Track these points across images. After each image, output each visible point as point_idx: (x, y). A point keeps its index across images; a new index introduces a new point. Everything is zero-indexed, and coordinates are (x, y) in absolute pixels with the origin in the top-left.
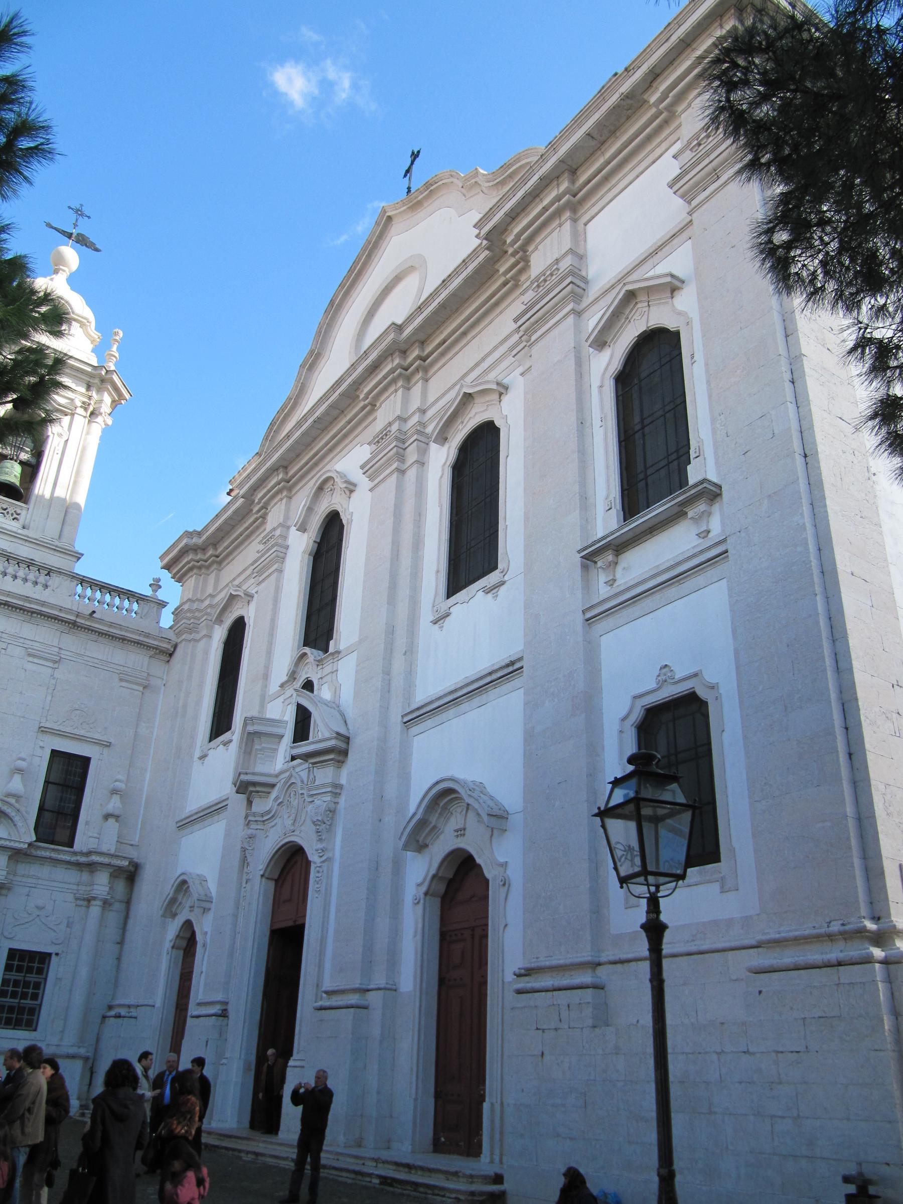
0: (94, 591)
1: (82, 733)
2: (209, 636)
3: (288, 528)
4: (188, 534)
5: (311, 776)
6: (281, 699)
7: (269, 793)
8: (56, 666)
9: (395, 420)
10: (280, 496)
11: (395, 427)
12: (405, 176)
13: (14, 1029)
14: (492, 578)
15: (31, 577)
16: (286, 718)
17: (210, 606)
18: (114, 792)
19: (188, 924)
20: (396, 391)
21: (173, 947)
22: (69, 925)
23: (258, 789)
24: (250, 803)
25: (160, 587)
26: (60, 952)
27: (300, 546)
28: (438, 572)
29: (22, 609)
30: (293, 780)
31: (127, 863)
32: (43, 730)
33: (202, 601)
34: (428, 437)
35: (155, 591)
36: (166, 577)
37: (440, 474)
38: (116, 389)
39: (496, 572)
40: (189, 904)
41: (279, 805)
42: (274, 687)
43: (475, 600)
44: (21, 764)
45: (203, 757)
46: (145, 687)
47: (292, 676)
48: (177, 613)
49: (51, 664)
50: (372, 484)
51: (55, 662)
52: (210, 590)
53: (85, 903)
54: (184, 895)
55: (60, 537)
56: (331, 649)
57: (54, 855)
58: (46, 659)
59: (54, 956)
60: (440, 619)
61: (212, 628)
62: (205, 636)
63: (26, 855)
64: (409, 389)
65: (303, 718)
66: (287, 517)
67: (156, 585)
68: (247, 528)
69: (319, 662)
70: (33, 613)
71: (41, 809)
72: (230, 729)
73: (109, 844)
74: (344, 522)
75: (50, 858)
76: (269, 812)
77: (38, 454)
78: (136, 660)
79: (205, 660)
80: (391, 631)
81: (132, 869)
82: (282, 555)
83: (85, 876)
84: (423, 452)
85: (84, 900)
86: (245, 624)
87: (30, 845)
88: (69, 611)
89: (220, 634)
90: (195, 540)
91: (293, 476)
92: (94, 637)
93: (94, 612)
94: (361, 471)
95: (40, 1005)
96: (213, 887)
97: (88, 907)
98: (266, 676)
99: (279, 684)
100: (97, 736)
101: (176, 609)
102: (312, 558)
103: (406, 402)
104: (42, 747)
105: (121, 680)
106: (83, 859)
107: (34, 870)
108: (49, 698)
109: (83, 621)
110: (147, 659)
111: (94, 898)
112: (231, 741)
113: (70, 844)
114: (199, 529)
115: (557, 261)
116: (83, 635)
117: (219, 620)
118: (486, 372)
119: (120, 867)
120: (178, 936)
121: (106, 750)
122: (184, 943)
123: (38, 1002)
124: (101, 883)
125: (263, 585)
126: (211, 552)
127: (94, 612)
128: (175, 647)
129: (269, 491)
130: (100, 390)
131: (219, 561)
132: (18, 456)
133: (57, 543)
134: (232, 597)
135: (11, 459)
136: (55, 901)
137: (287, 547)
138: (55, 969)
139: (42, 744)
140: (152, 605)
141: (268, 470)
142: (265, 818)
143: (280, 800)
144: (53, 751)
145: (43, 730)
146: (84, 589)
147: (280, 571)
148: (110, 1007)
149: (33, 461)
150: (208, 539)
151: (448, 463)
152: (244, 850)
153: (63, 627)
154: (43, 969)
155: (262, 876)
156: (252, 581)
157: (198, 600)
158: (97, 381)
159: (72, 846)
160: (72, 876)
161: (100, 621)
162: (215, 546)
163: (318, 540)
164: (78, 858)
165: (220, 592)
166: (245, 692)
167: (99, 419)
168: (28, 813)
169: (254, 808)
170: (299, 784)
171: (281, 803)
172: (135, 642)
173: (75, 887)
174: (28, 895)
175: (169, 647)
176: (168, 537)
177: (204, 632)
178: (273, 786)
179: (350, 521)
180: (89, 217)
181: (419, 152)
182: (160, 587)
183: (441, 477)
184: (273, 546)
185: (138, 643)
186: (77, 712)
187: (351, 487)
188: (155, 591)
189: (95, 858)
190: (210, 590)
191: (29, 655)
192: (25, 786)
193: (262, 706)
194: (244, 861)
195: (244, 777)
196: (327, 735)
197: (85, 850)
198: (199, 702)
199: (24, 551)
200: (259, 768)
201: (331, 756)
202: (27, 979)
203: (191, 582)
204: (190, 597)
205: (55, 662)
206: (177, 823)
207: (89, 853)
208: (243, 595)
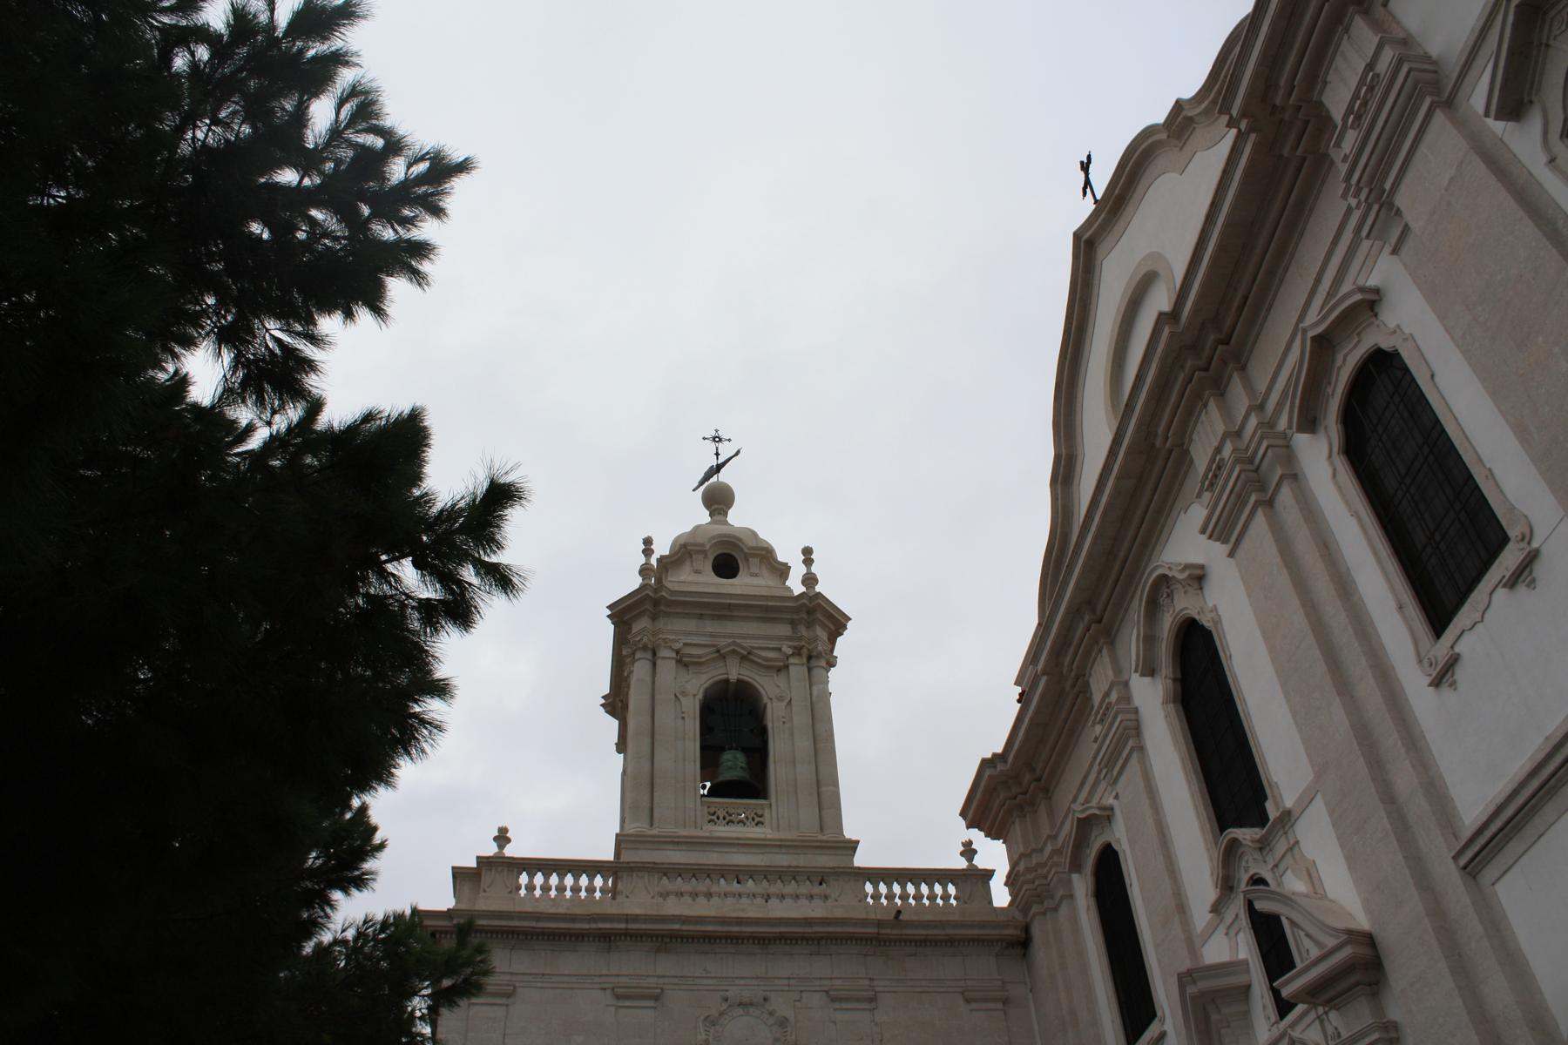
2: (1071, 896)
3: (1126, 684)
5: (1330, 1030)
6: (1222, 930)
8: (873, 1005)
9: (1222, 442)
11: (1227, 450)
12: (1085, 194)
14: (1509, 560)
16: (1242, 955)
17: (1055, 852)
20: (1205, 406)
25: (975, 852)
28: (1400, 607)
33: (1041, 850)
34: (1284, 435)
37: (1330, 471)
39: (1511, 546)
42: (1201, 915)
43: (1494, 619)
46: (1005, 1002)
47: (1227, 885)
48: (1011, 881)
50: (1226, 548)
52: (1046, 831)
55: (822, 829)
56: (1272, 812)
58: (858, 1000)
60: (1443, 675)
61: (1070, 882)
62: (1062, 898)
64: (1222, 395)
65: (1271, 937)
66: (1118, 670)
67: (969, 851)
69: (1263, 845)
70: (819, 940)
72: (1154, 1015)
74: (1207, 625)
80: (1364, 735)
84: (1289, 457)
86: (1115, 853)
89: (1082, 886)
90: (1000, 767)
94: (1204, 537)
98: (1182, 908)
99: (1208, 907)
101: (1008, 876)
103: (1226, 413)
112: (1163, 1035)
114: (999, 750)
115: (1370, 67)
117: (1076, 866)
118: (1330, 295)
125: (1123, 779)
126: (1027, 777)
128: (1027, 929)
130: (809, 625)
133: (820, 837)
137: (1136, 711)
141: (1068, 611)
147: (1141, 748)
150: (1016, 757)
151: (1335, 449)
156: (1103, 785)
157: (1034, 851)
165: (1063, 823)
166: (1157, 947)
177: (1060, 893)
179: (1218, 621)
181: (1089, 157)
182: (975, 852)
183: (1334, 475)
184: (1115, 718)
187: (1198, 572)
190: (1046, 831)
191: (833, 1000)
193: (1193, 951)
196: (1331, 942)
199: (783, 860)
201: (1352, 979)
203: (1017, 830)
204: (1022, 849)
205: (872, 1000)
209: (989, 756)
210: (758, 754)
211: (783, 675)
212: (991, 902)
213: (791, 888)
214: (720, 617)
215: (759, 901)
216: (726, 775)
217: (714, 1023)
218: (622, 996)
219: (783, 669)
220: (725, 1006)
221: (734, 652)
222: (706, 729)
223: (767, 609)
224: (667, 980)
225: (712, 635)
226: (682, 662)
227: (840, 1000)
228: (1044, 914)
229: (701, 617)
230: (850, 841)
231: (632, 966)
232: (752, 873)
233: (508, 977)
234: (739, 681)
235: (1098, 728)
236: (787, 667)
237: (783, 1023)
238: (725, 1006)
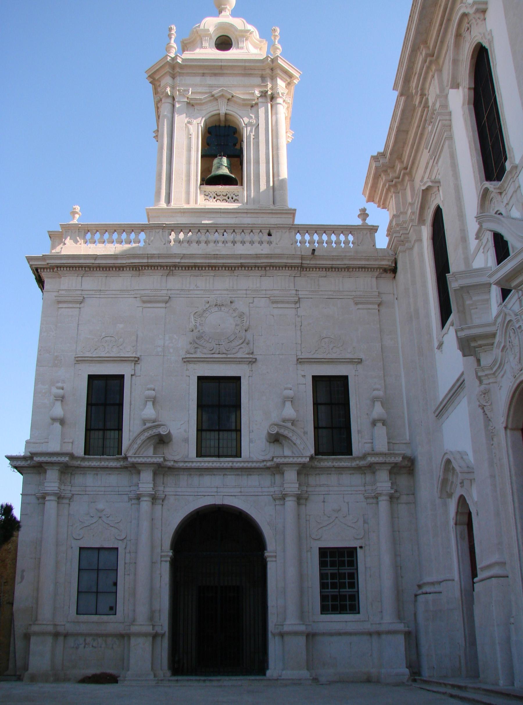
0: (311, 235)
1: (334, 356)
2: (420, 240)
3: (446, 96)
4: (375, 158)
7: (492, 344)
8: (298, 305)
10: (431, 74)
13: (340, 613)
15: (256, 238)
17: (413, 213)
18: (374, 400)
19: (462, 501)
21: (456, 524)
22: (365, 522)
23: (480, 342)
24: (478, 361)
25: (367, 215)
26: (363, 546)
27: (458, 102)
29: (257, 267)
30: (508, 319)
31: (401, 459)
32: (300, 361)
35: (364, 220)
36: (372, 208)
38: (286, 72)
40: (459, 481)
41: (502, 351)
44: (290, 393)
45: (440, 345)
49: (293, 306)
51: (296, 303)
53: (374, 501)
54: (453, 474)
57: (336, 464)
58: (288, 302)
59: (359, 550)
63: (312, 467)
67: (364, 214)
68: (418, 126)
71: (316, 428)
73: (382, 446)
75: (334, 467)
76: (495, 361)
78: (365, 283)
79: (422, 261)
81: (409, 464)
82: (447, 123)
83: (369, 478)
85: (373, 498)
86: (441, 209)
87: (311, 458)
88: (293, 257)
89: (426, 232)
91: (435, 46)
92: (324, 273)
93: (314, 250)
95: (358, 591)
96: (471, 457)
97: (377, 503)
98: (464, 239)
99: (475, 237)
100: (348, 356)
102: (472, 107)
104: (304, 376)
105: (356, 304)
106: (362, 463)
107: (323, 479)
108: (299, 333)
109: (308, 262)
110: (374, 280)
111: (380, 494)
113: (348, 451)
114: (382, 150)
116: (314, 274)
117: (421, 221)
119: (396, 464)
120: (457, 513)
121: (359, 366)
122: (466, 519)
123: (356, 590)
124: (383, 482)
126: (398, 166)
129: (420, 75)
131: (408, 172)
133: (272, 207)
134: (426, 192)
136: (348, 503)
137: (450, 114)
138: (363, 560)
139: (303, 374)
140: (365, 232)
142: (494, 369)
143: (502, 345)
144: (314, 377)
145: (300, 361)
146: (303, 236)
147: (451, 138)
148: (420, 586)
150: (391, 154)
152: (483, 407)
153: (294, 272)
154: (353, 561)
155: (506, 428)
157: (401, 213)
158: (268, 71)
159: (352, 455)
160: (357, 479)
161: (322, 258)
162: (400, 158)
163: (473, 86)
164: (358, 462)
167: (280, 100)
168: (305, 433)
169: (483, 363)
170: (513, 318)
171: (504, 347)
172: (359, 268)
173: (362, 488)
174: (324, 502)
175: (390, 263)
176: (360, 170)
178: (494, 335)
182: (367, 215)
185: (362, 268)
186: (326, 340)
188: (364, 220)
189: (371, 459)
190: (409, 200)
191: (273, 302)
192: (297, 411)
194: (487, 420)
195: (462, 334)
197: (361, 455)
198: (426, 301)
200: (476, 322)
202: (341, 571)
205: (296, 303)
206: (434, 412)
207: (364, 457)
208: (429, 184)
209: (375, 154)
210: (236, 157)
212: (374, 245)
213: (248, 238)
214: (215, 75)
215: (230, 245)
217: (201, 316)
218: (148, 301)
219: (254, 106)
220: (208, 305)
221: (222, 96)
223: (245, 68)
224: (173, 292)
225: (211, 86)
227: (277, 302)
228: (405, 251)
229: (203, 75)
230: (291, 210)
231: (151, 282)
233: (80, 292)
235: (430, 127)
237: (241, 315)
238: (208, 305)
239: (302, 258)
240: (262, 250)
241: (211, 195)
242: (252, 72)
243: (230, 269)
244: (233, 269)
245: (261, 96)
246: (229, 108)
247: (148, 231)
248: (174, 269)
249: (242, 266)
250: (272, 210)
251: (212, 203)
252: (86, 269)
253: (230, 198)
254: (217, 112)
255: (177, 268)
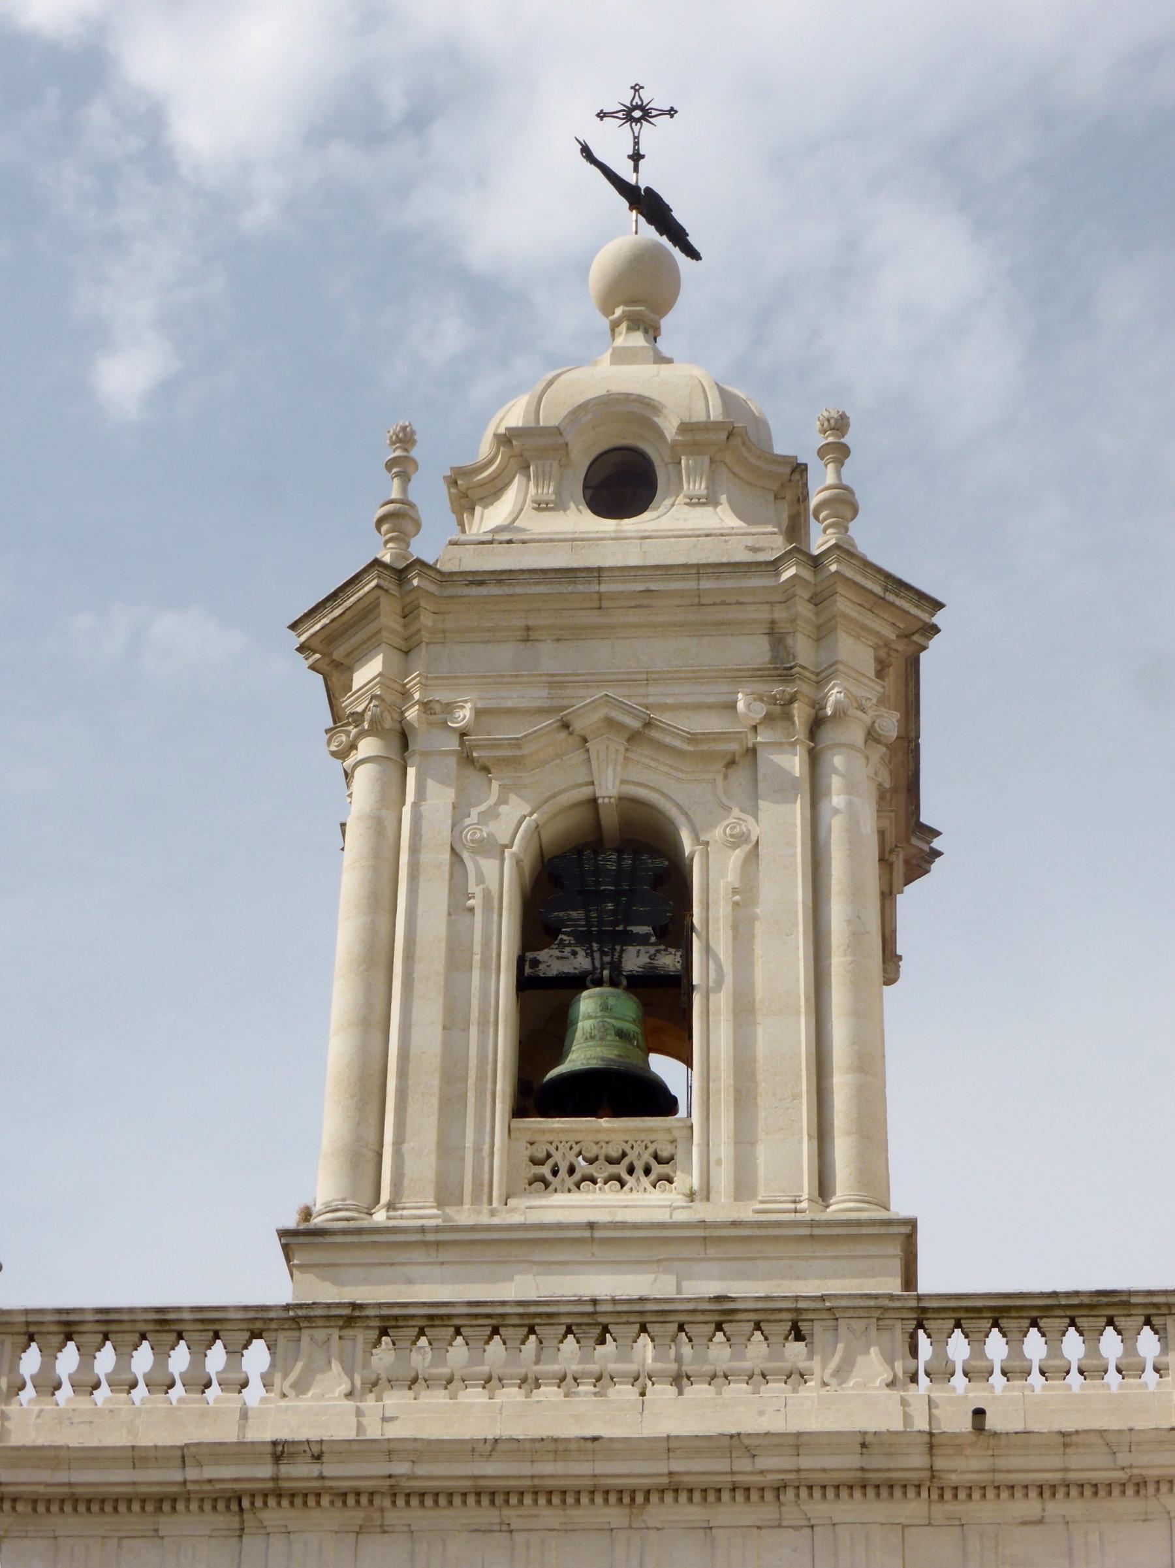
70: (779, 1489)
77: (676, 930)
93: (979, 1413)
127: (979, 1413)
132: (616, 967)
135: (598, 983)
149: (669, 961)
180: (671, 112)
211: (740, 775)
216: (581, 1055)
222: (538, 925)
225: (555, 683)
226: (472, 760)
232: (643, 1318)
234: (628, 803)
236: (752, 752)
239: (932, 1442)
240: (761, 1413)
241: (557, 1157)
242: (732, 613)
243: (626, 1500)
244: (640, 1498)
245: (769, 718)
246: (636, 774)
247: (282, 1338)
248: (387, 1502)
249: (675, 1488)
250: (812, 1224)
251: (559, 1199)
252: (20, 1507)
253: (639, 1171)
254: (585, 792)
255: (401, 1501)
